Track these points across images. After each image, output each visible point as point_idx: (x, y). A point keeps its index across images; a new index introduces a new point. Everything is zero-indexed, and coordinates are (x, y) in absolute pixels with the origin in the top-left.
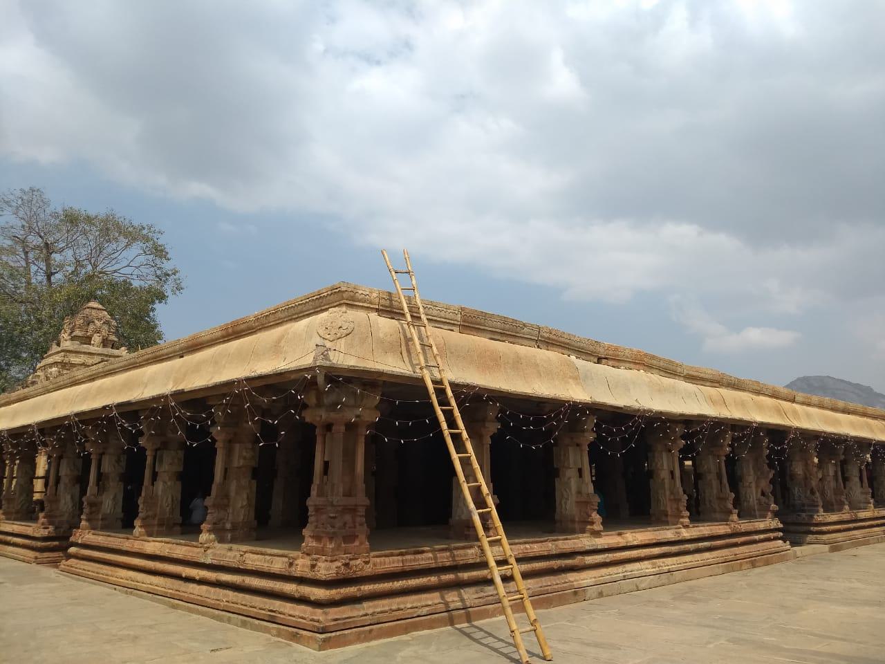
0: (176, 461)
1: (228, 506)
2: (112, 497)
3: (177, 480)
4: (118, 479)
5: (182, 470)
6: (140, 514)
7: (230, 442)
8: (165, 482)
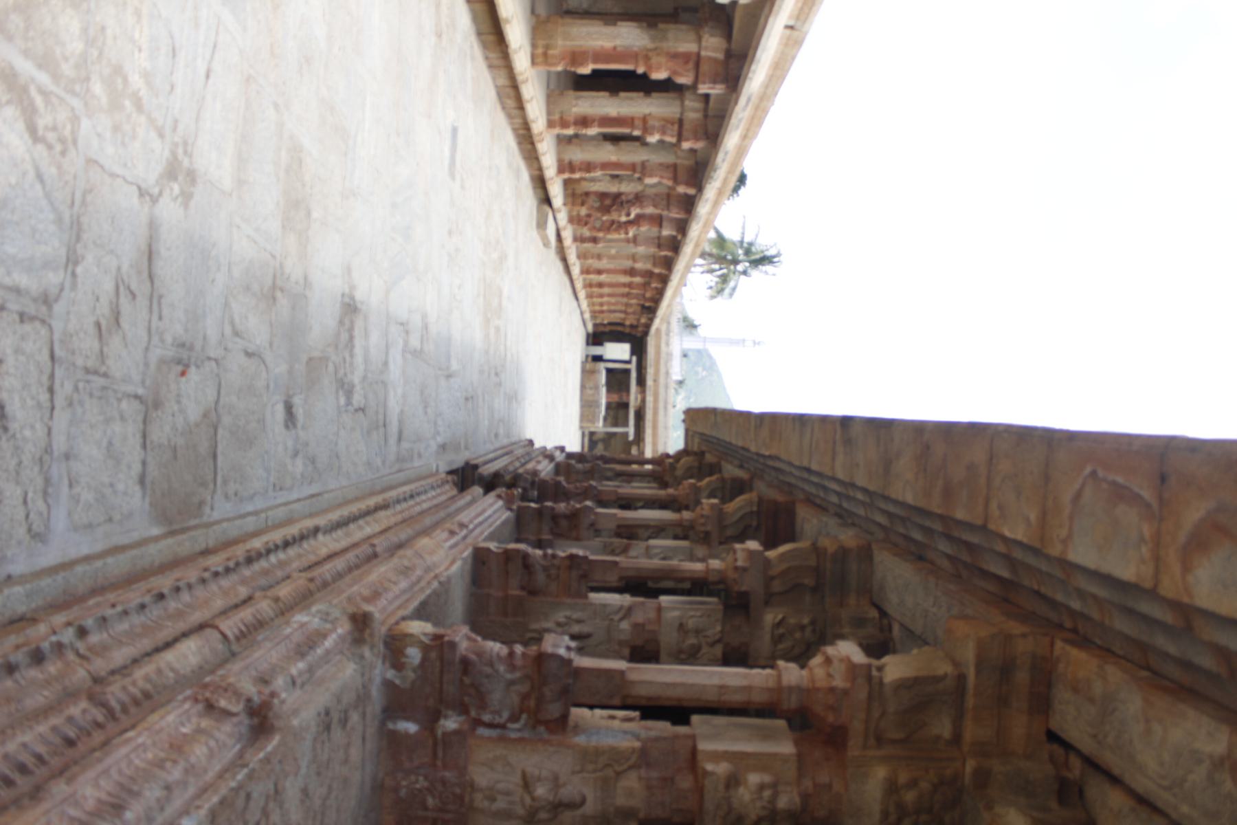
0: (692, 640)
1: (537, 721)
6: (539, 552)
8: (628, 612)
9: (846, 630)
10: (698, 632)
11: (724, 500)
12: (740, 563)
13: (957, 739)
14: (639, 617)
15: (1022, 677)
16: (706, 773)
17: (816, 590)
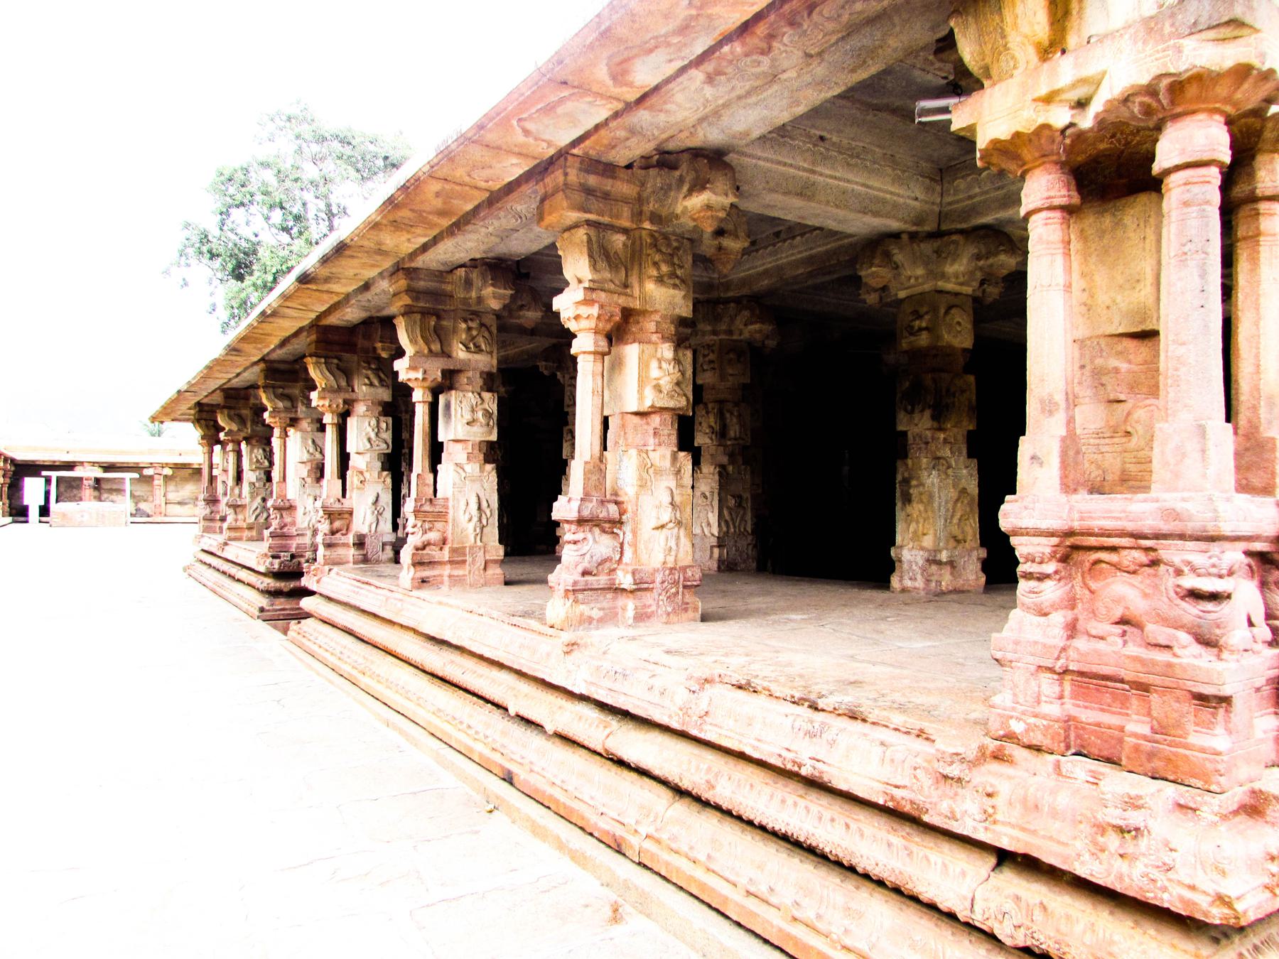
0: (480, 414)
1: (620, 523)
2: (372, 499)
3: (487, 461)
4: (379, 464)
5: (494, 437)
7: (618, 331)
9: (474, 294)
10: (473, 411)
11: (314, 388)
12: (420, 375)
13: (625, 231)
14: (462, 458)
15: (592, 180)
16: (652, 406)
17: (439, 317)
